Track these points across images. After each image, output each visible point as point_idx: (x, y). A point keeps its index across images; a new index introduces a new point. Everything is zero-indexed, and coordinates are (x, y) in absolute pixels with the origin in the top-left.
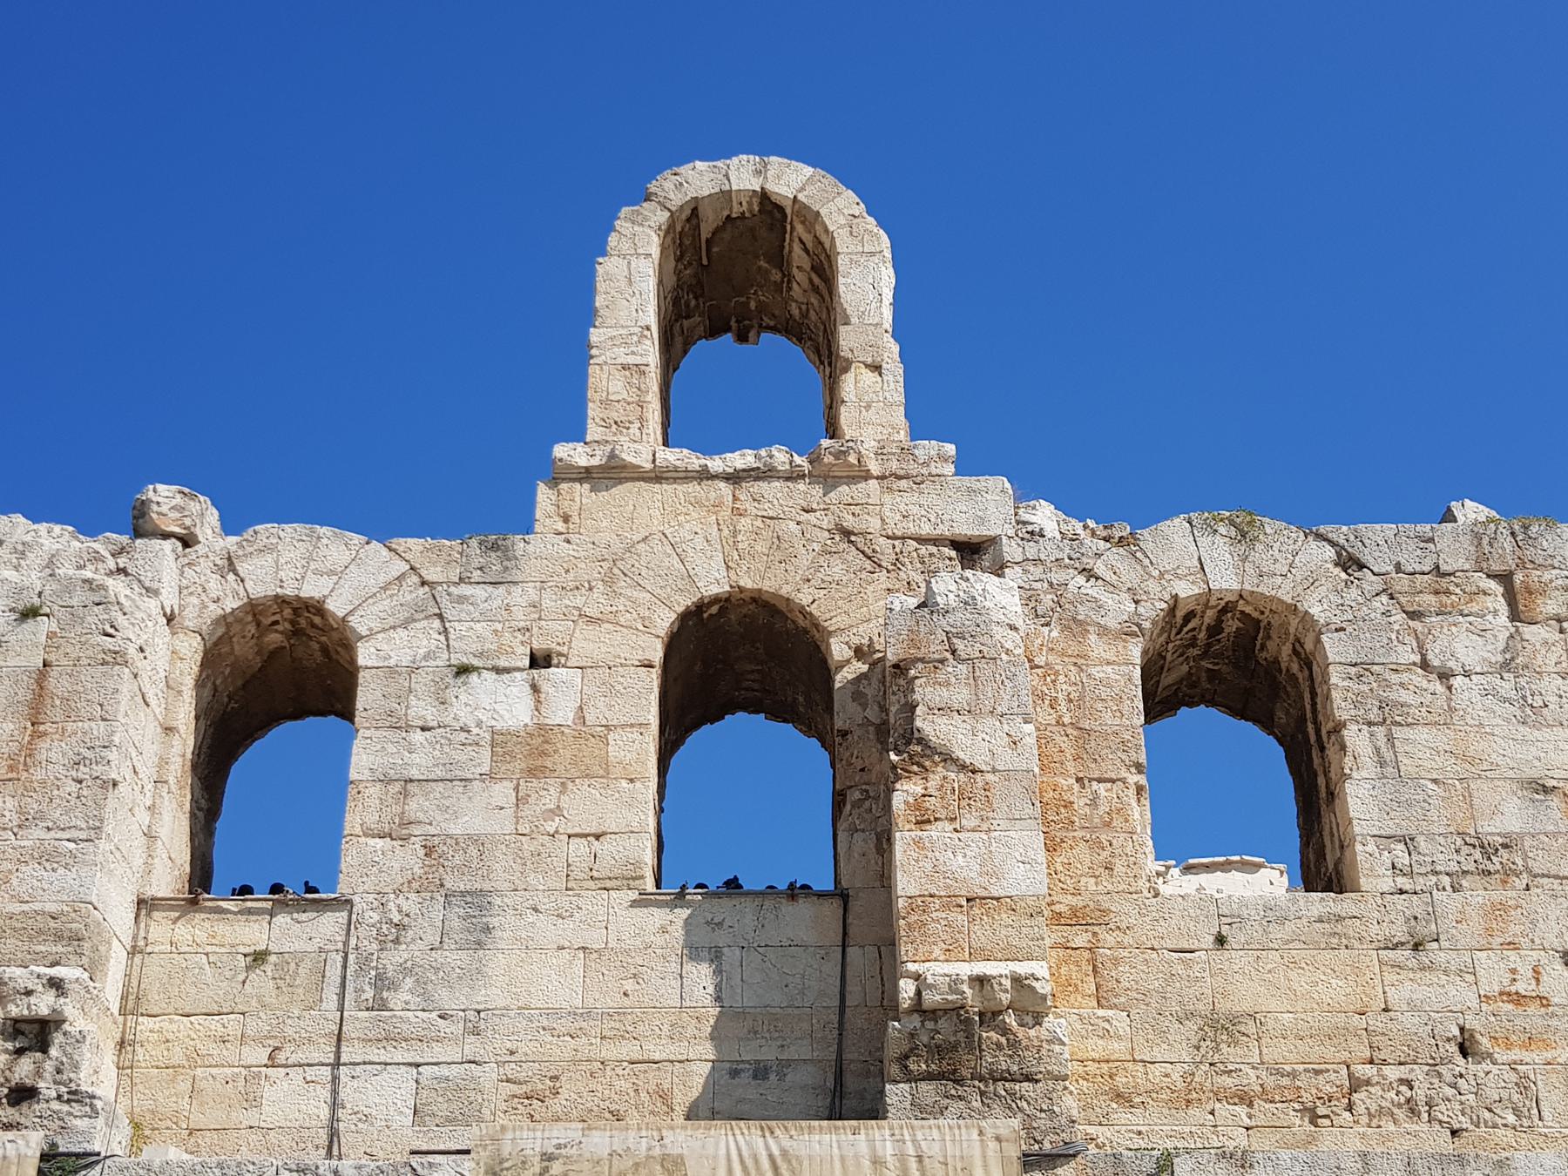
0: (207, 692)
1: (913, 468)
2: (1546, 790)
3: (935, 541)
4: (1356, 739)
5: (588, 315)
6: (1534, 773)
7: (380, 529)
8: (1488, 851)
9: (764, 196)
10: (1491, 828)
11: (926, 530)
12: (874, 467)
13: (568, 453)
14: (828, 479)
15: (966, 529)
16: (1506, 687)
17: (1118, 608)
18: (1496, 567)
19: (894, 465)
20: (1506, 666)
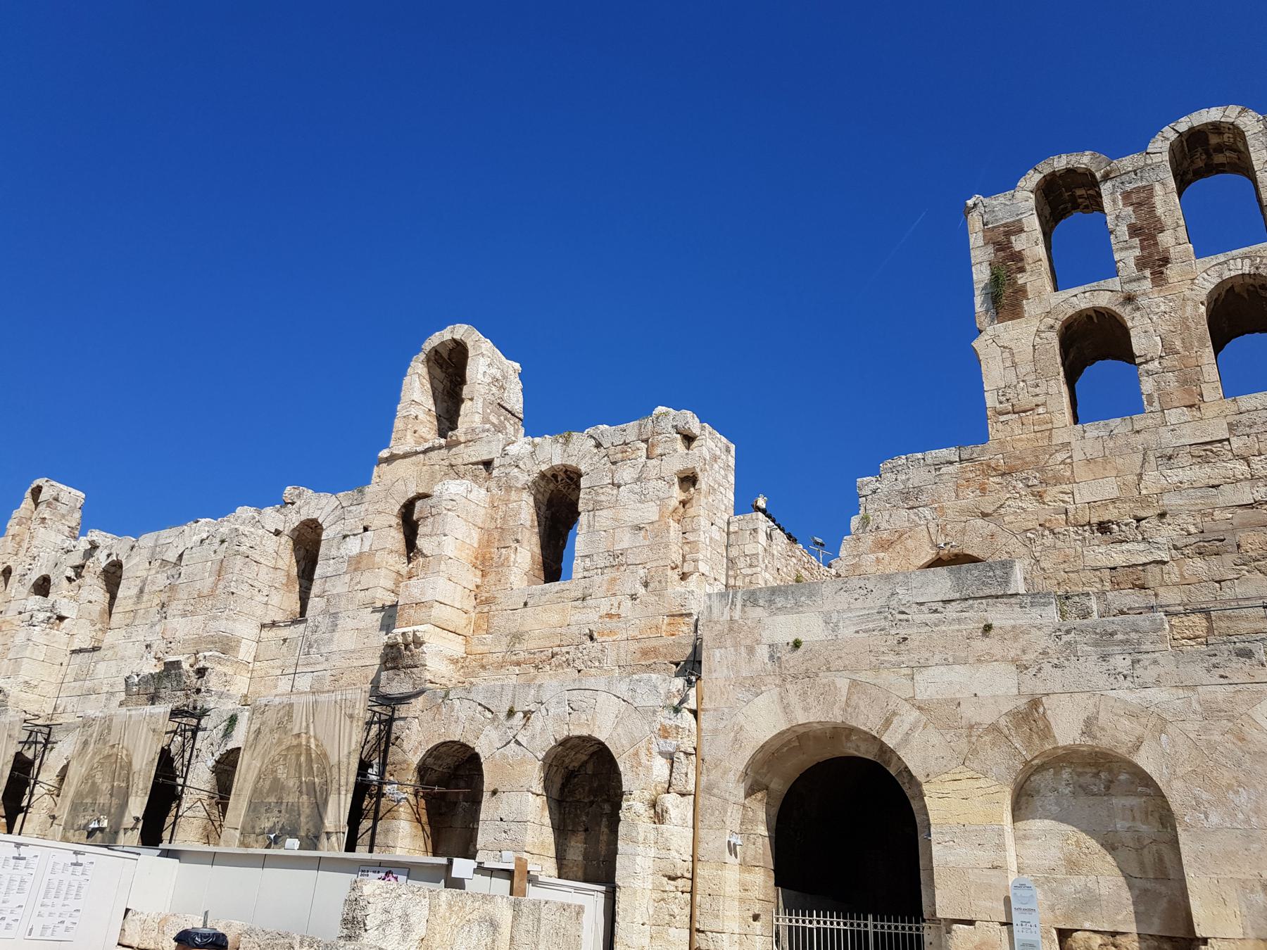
0: (302, 552)
1: (475, 437)
2: (640, 529)
3: (477, 463)
4: (583, 519)
5: (397, 400)
6: (636, 522)
7: (334, 492)
8: (615, 557)
9: (454, 340)
10: (618, 548)
11: (475, 460)
12: (462, 439)
13: (384, 453)
14: (449, 446)
15: (486, 457)
16: (636, 488)
17: (524, 479)
18: (644, 437)
19: (469, 437)
20: (638, 479)
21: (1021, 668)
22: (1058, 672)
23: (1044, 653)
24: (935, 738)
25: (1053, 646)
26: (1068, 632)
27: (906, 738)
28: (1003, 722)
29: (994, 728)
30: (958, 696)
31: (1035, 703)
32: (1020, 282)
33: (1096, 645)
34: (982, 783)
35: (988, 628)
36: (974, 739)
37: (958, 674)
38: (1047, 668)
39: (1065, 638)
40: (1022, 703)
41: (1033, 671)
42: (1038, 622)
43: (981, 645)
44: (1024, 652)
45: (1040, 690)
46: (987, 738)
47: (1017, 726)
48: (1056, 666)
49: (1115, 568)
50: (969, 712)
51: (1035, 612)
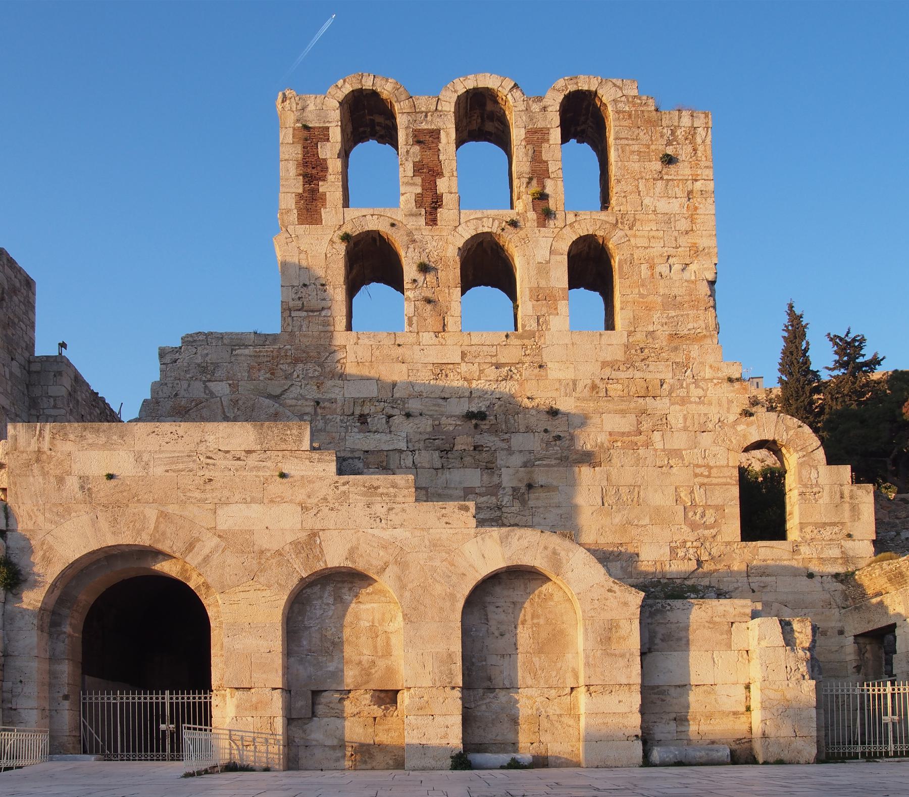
21: (304, 508)
22: (334, 514)
23: (325, 499)
24: (232, 560)
25: (330, 492)
26: (344, 484)
27: (206, 559)
28: (287, 548)
29: (279, 553)
30: (254, 528)
31: (313, 535)
32: (321, 190)
33: (364, 495)
34: (267, 593)
35: (283, 475)
36: (263, 561)
37: (255, 510)
38: (325, 510)
39: (342, 488)
40: (302, 536)
41: (314, 511)
42: (323, 474)
43: (277, 487)
44: (309, 497)
45: (318, 526)
46: (274, 561)
47: (298, 554)
48: (332, 509)
49: (367, 452)
50: (263, 541)
51: (320, 466)
